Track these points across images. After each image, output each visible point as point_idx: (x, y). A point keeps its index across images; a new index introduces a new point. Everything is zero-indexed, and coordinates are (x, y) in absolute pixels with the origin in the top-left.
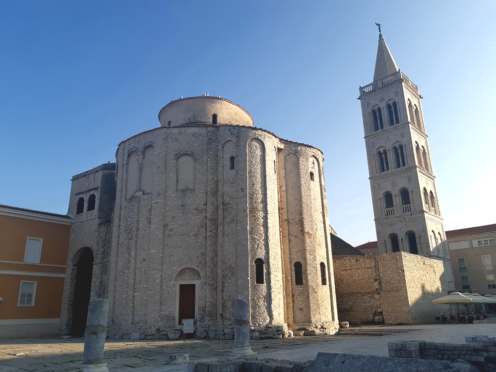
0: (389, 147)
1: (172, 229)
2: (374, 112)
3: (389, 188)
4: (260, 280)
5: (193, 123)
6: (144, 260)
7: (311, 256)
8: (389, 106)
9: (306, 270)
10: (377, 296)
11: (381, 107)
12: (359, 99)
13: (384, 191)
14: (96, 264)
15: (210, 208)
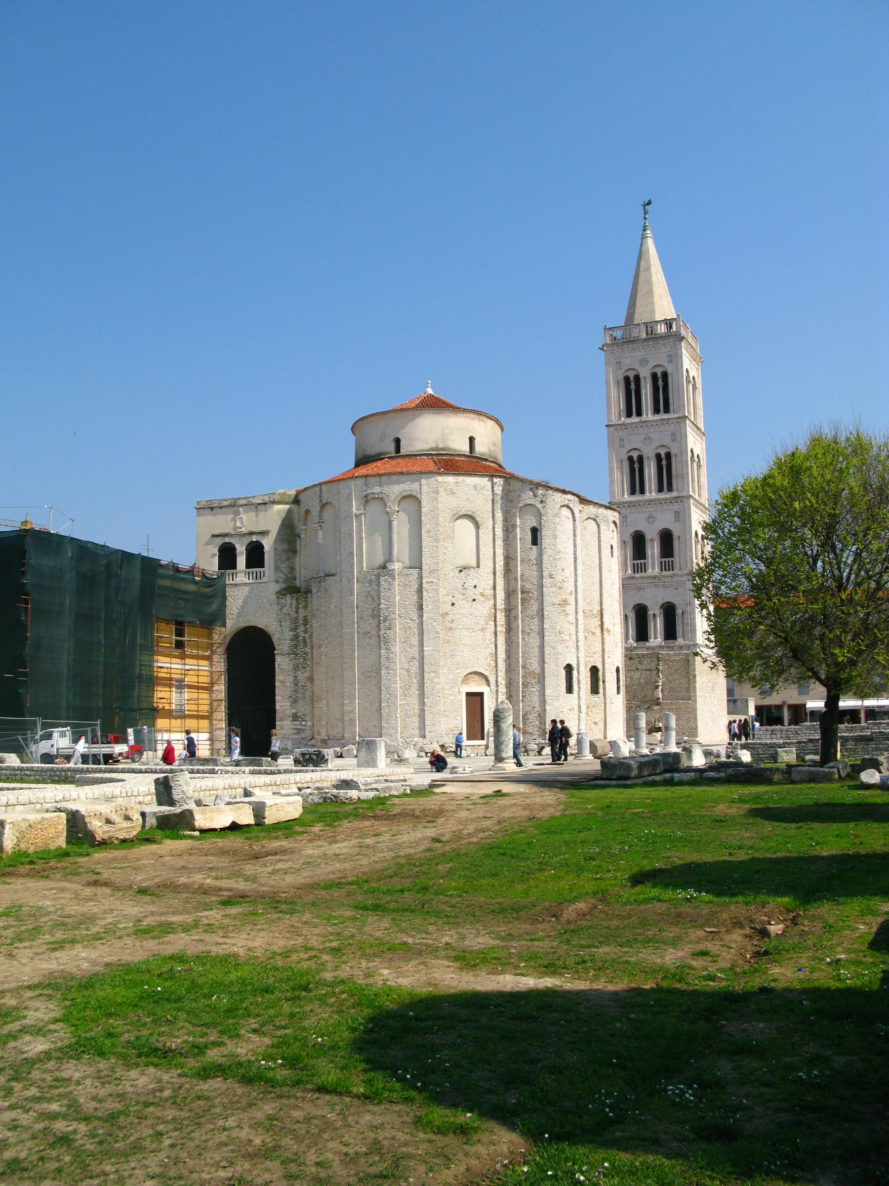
0: (649, 453)
1: (453, 621)
2: (627, 380)
3: (642, 527)
4: (569, 690)
5: (442, 449)
6: (414, 658)
7: (610, 660)
8: (654, 376)
9: (604, 676)
10: (656, 708)
11: (641, 376)
12: (602, 349)
13: (632, 530)
14: (281, 654)
15: (501, 595)
